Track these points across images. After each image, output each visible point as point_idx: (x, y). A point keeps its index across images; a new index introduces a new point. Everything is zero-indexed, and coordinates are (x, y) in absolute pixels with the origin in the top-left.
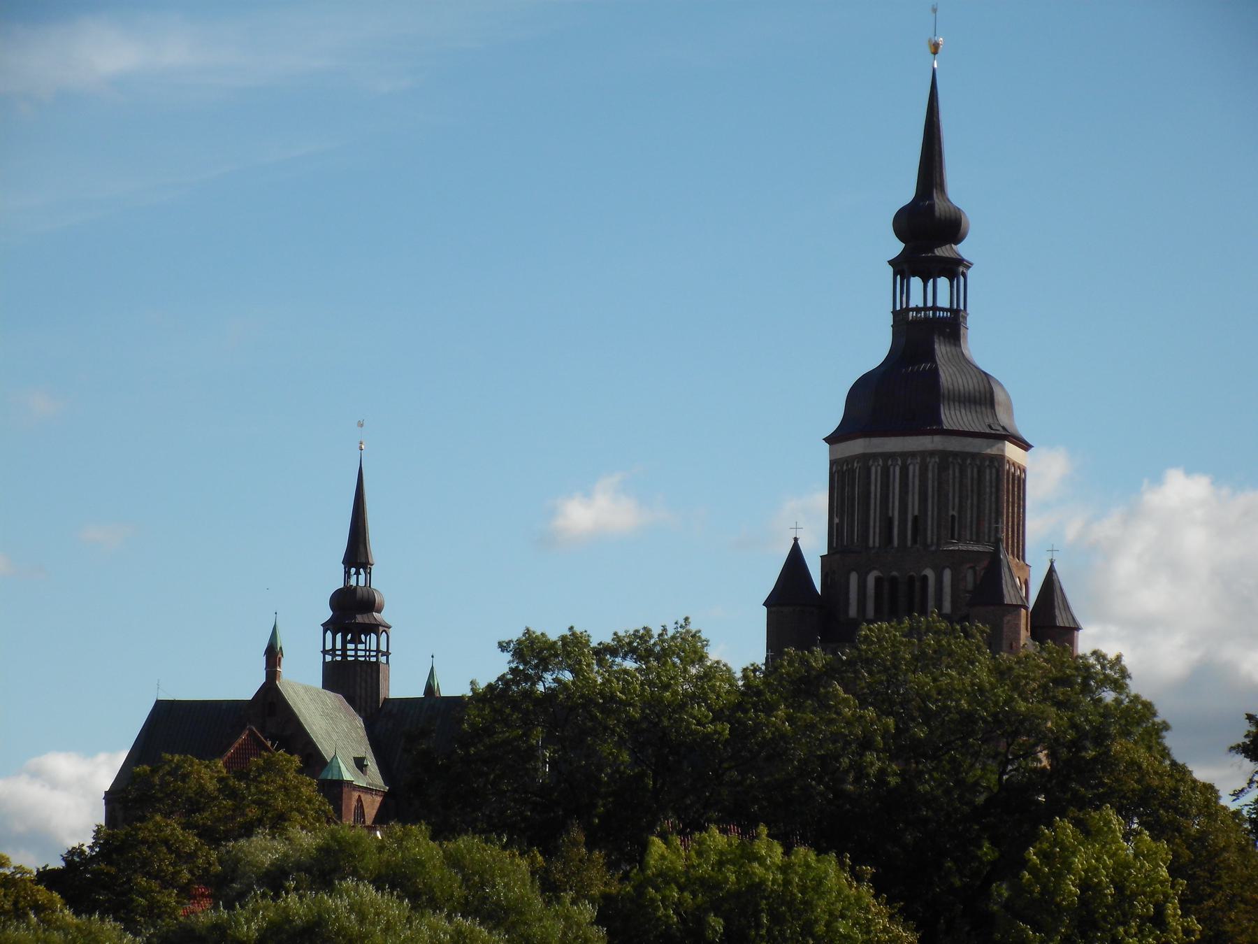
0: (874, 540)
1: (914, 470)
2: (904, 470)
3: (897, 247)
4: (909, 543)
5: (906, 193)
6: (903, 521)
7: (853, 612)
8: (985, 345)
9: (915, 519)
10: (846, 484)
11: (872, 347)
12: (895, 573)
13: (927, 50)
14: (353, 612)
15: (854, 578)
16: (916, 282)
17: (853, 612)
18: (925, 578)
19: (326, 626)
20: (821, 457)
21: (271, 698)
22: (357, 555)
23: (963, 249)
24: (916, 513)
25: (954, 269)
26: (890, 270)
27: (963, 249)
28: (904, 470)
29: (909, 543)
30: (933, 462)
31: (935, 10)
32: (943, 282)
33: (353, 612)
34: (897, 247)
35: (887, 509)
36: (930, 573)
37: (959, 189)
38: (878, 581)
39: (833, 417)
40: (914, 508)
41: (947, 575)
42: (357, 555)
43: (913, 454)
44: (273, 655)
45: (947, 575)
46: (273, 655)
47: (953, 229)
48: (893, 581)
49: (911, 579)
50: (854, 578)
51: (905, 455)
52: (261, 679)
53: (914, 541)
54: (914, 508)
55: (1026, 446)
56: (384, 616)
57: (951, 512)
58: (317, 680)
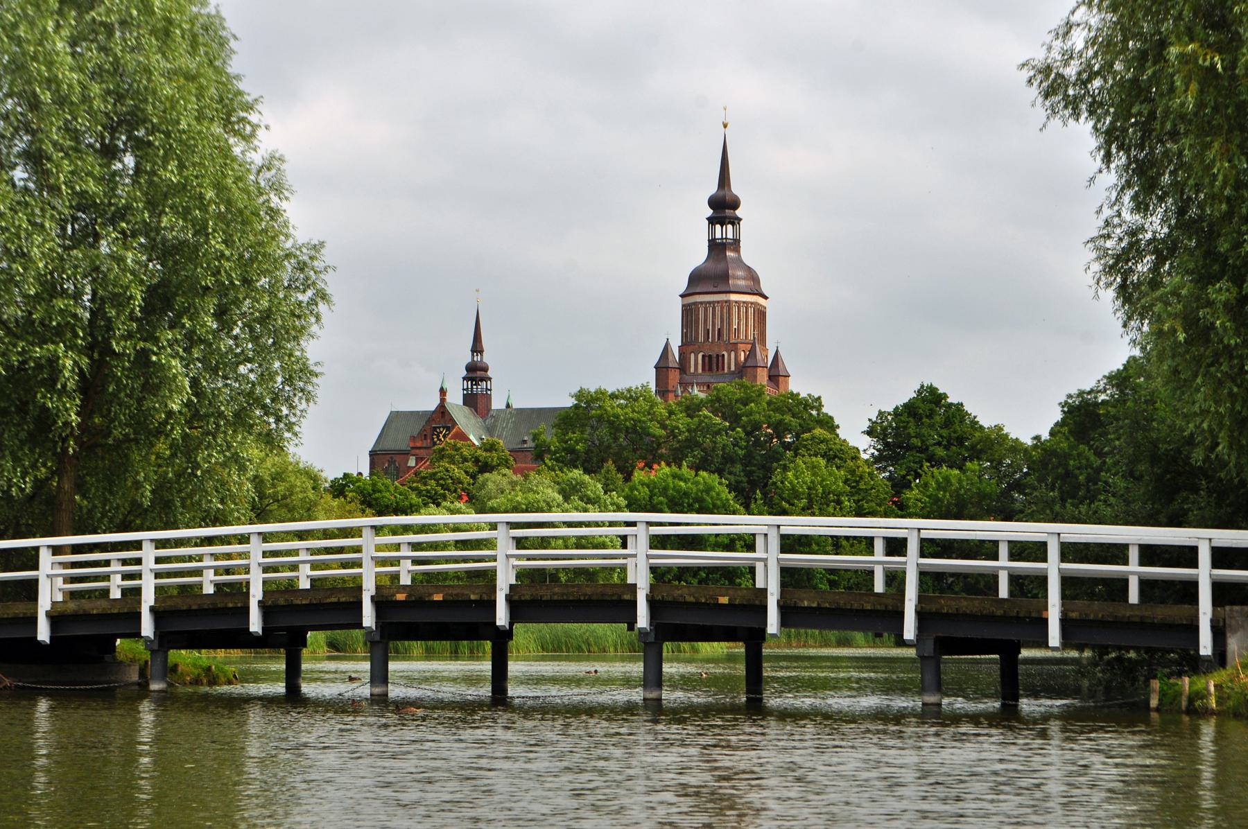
0: (701, 339)
1: (718, 309)
3: (710, 212)
5: (713, 188)
7: (692, 370)
8: (749, 254)
10: (689, 314)
11: (699, 255)
14: (476, 373)
15: (692, 356)
16: (718, 227)
17: (692, 370)
19: (464, 379)
20: (678, 303)
21: (442, 410)
22: (477, 348)
23: (739, 213)
25: (735, 221)
27: (739, 213)
32: (730, 227)
33: (476, 373)
34: (710, 212)
37: (736, 188)
39: (683, 285)
40: (718, 326)
41: (733, 354)
42: (477, 348)
44: (443, 392)
45: (733, 354)
46: (443, 392)
47: (735, 204)
48: (710, 357)
50: (692, 356)
51: (714, 302)
52: (438, 402)
54: (718, 326)
55: (766, 298)
56: (490, 374)
58: (461, 402)
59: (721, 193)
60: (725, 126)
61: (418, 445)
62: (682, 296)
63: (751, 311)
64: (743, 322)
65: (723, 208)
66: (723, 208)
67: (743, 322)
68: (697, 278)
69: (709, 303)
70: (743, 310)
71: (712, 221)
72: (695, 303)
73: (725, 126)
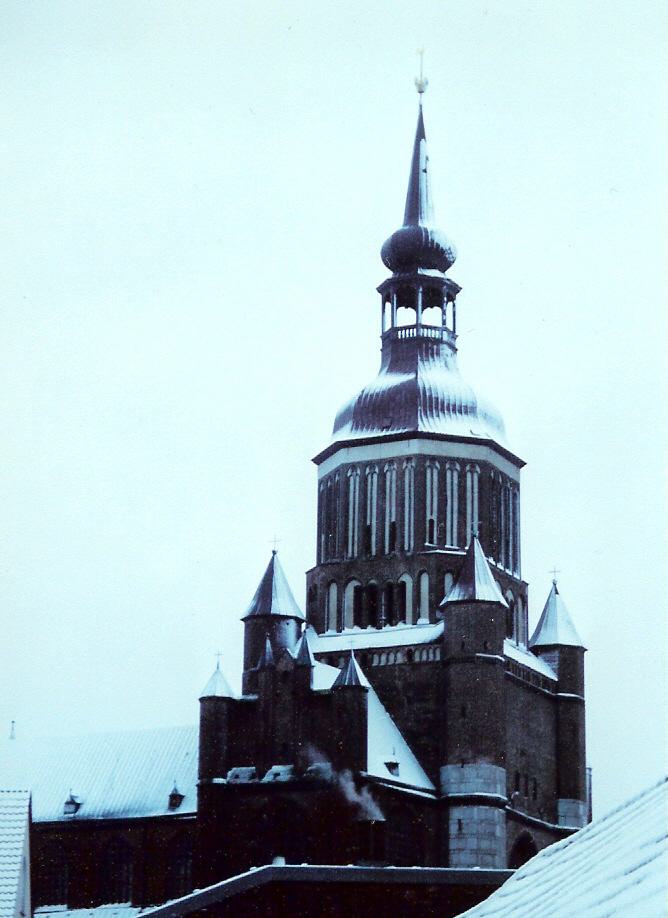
4: (387, 551)
5: (396, 223)
6: (381, 528)
9: (393, 525)
10: (332, 503)
12: (373, 581)
13: (415, 89)
15: (334, 589)
18: (403, 584)
24: (393, 520)
26: (379, 297)
28: (382, 476)
29: (387, 551)
30: (409, 469)
31: (421, 53)
35: (365, 518)
36: (407, 579)
38: (357, 590)
40: (391, 516)
49: (390, 587)
50: (334, 589)
51: (381, 463)
53: (392, 548)
54: (391, 516)
57: (428, 517)
59: (407, 228)
60: (421, 92)
62: (318, 460)
63: (472, 481)
64: (453, 504)
65: (415, 268)
66: (415, 268)
67: (453, 504)
69: (370, 464)
70: (452, 478)
71: (387, 291)
73: (421, 92)
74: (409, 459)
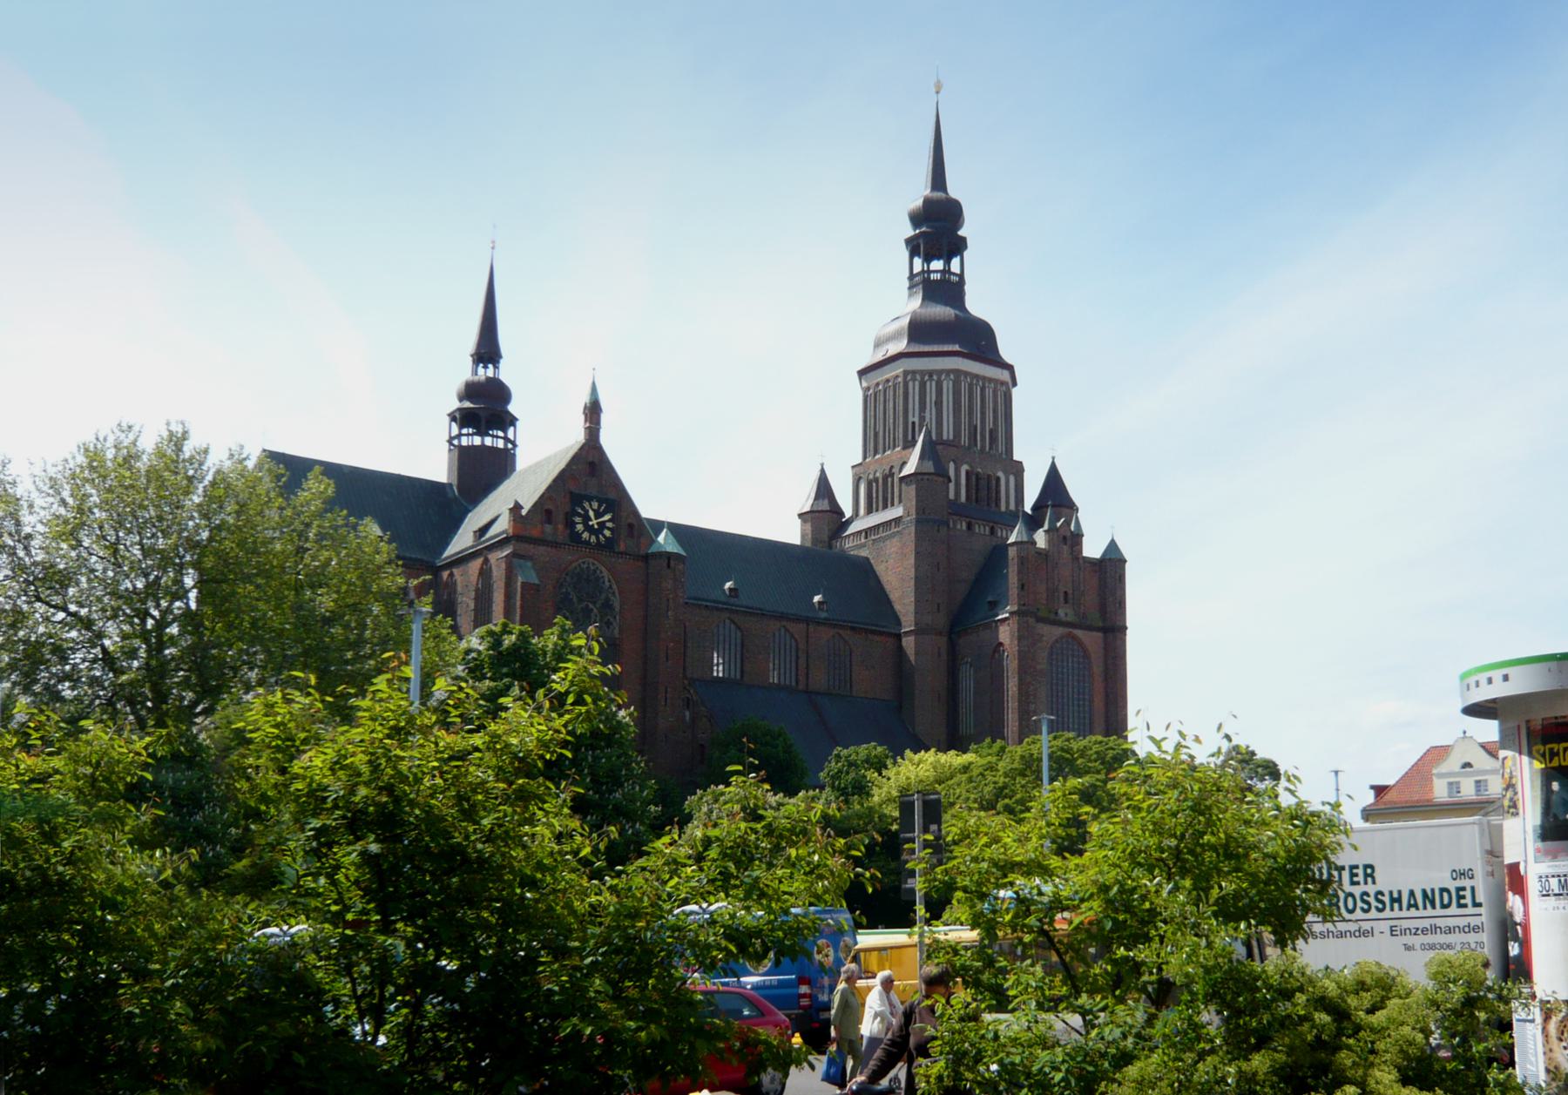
0: (964, 440)
1: (989, 393)
2: (983, 390)
3: (910, 232)
5: (917, 192)
7: (952, 496)
9: (991, 431)
17: (952, 496)
18: (998, 479)
28: (983, 390)
36: (1000, 474)
40: (989, 424)
43: (991, 380)
48: (977, 475)
50: (952, 465)
51: (984, 378)
54: (989, 424)
61: (535, 533)
65: (938, 229)
66: (938, 229)
68: (918, 330)
69: (977, 377)
72: (957, 372)
74: (1003, 383)
